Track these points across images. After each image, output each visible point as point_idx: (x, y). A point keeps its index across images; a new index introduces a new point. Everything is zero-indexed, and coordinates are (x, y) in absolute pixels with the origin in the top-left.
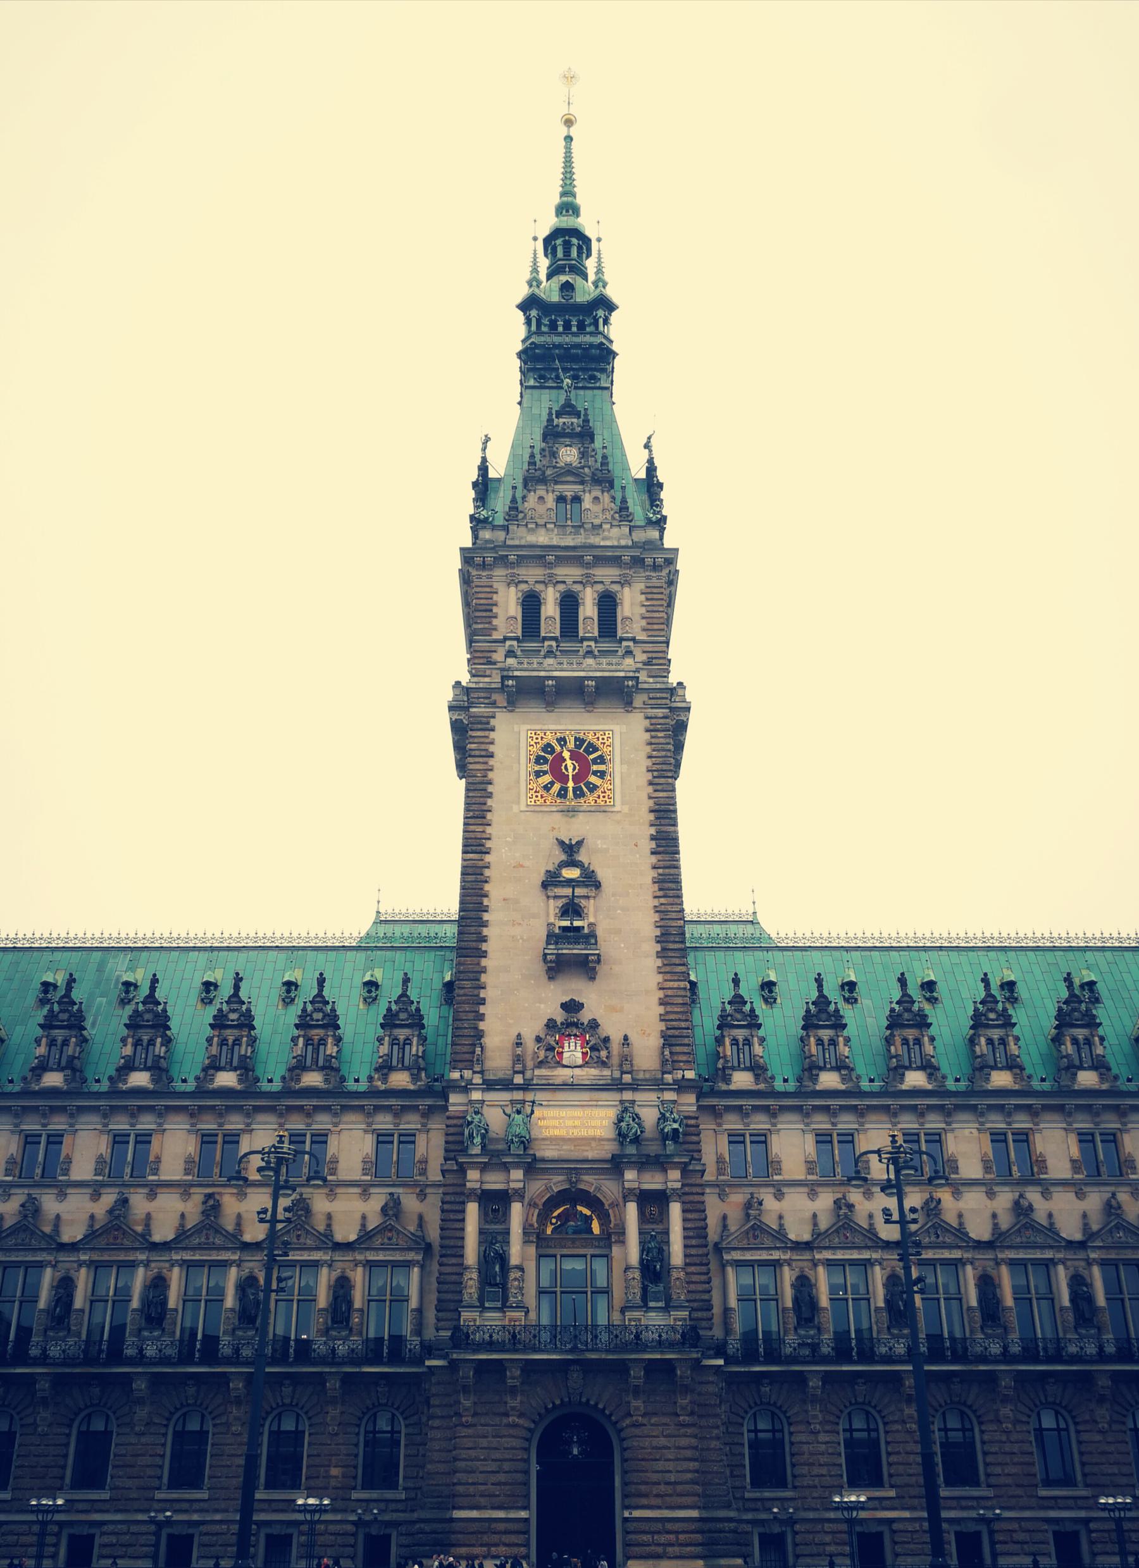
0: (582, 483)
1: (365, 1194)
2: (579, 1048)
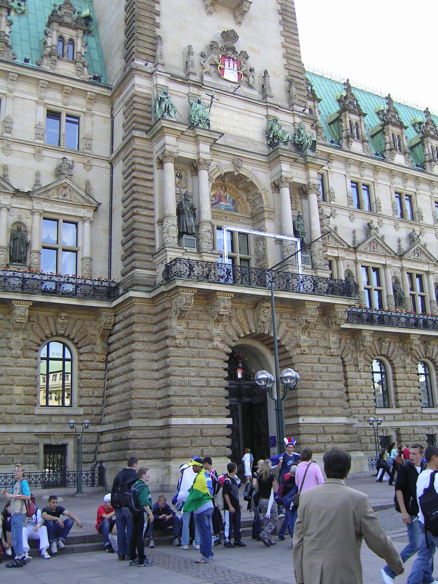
1: (38, 155)
2: (236, 69)
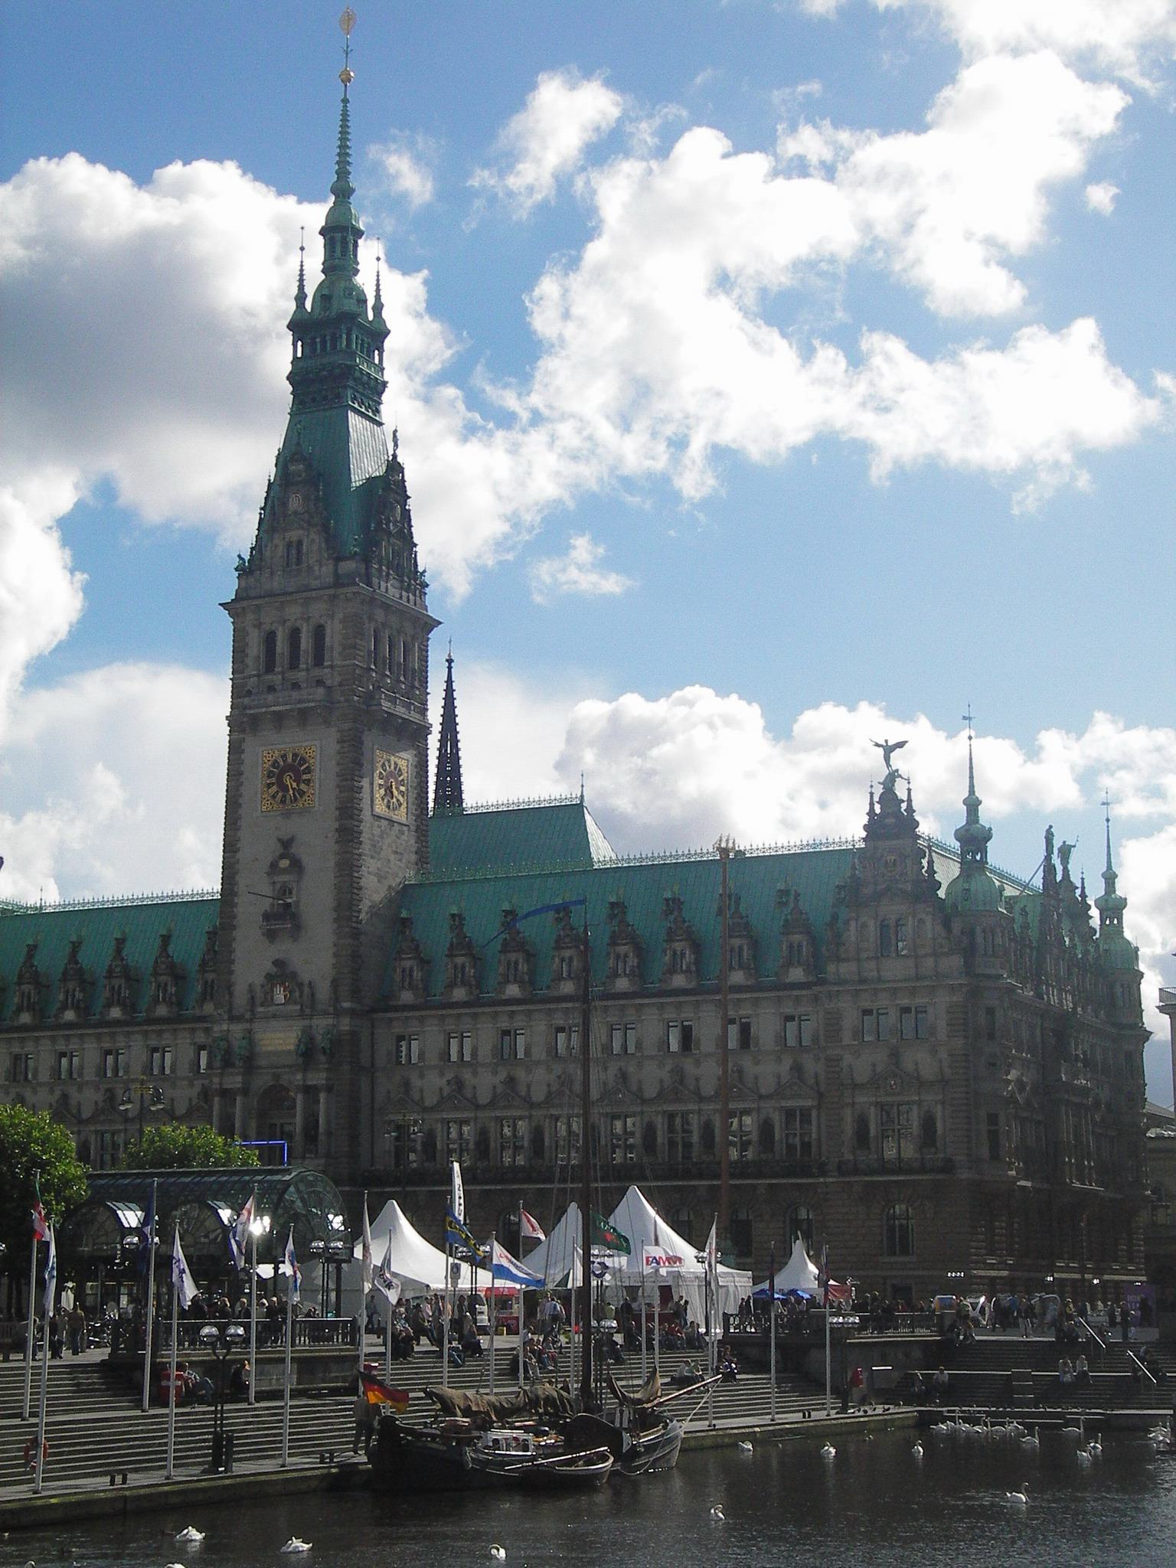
1: (191, 1085)
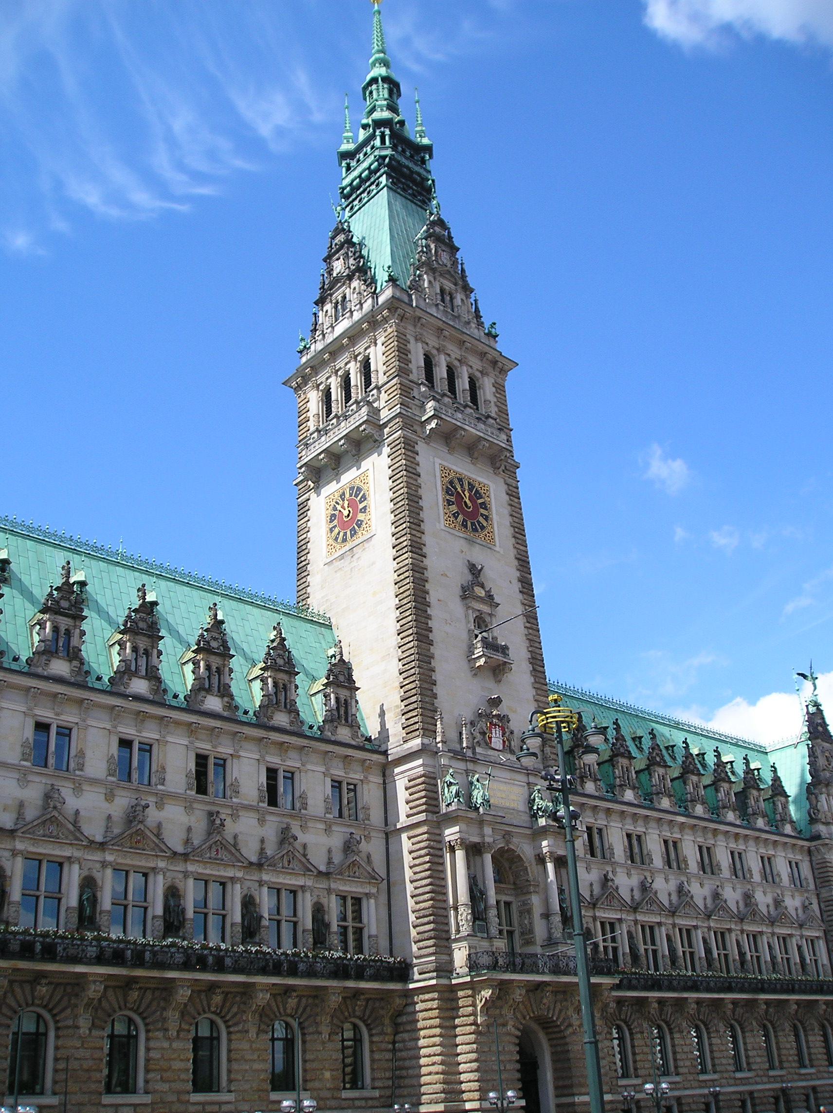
0: (456, 284)
